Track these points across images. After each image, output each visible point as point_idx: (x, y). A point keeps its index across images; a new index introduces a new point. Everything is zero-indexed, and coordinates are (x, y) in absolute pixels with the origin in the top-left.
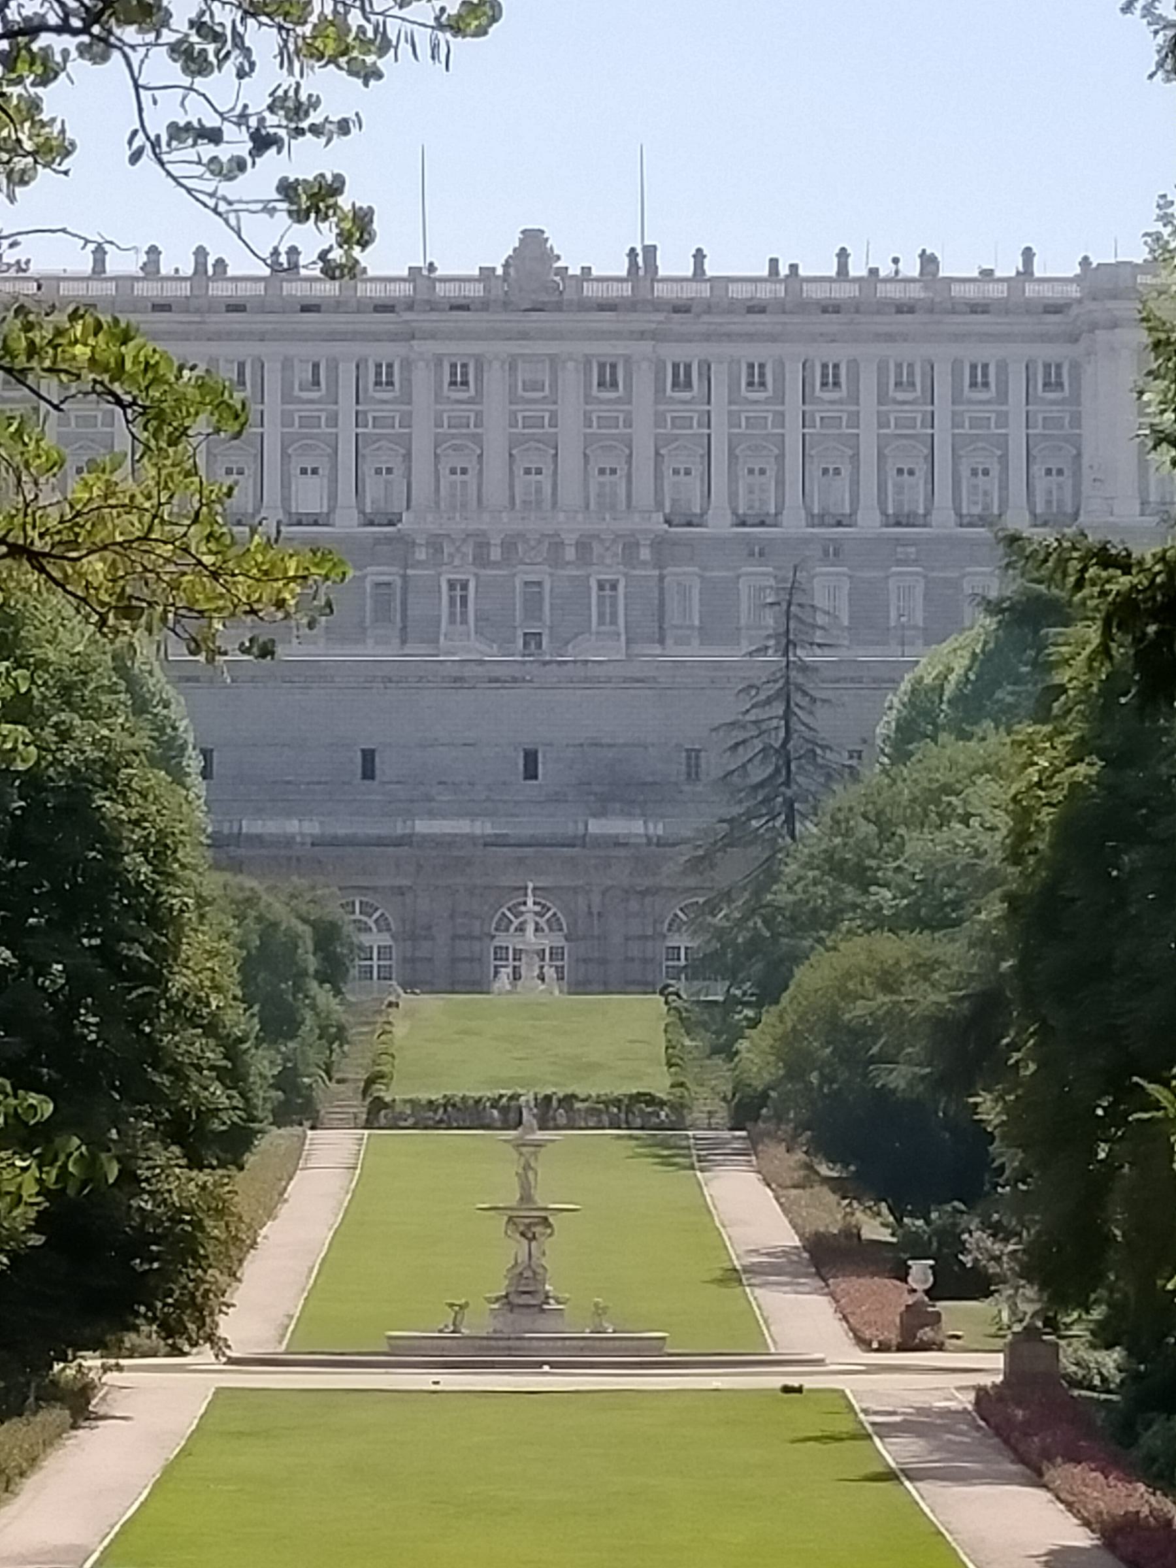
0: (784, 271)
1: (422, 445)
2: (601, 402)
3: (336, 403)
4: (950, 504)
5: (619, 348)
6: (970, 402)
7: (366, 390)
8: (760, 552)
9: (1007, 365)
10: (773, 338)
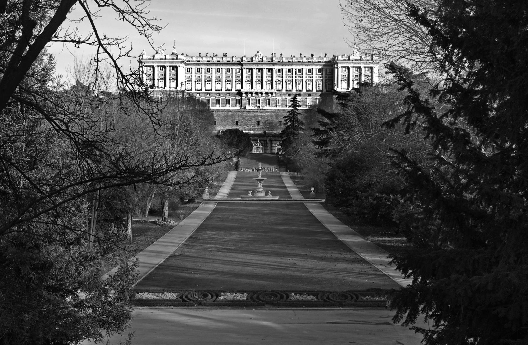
0: (293, 56)
8: (290, 95)
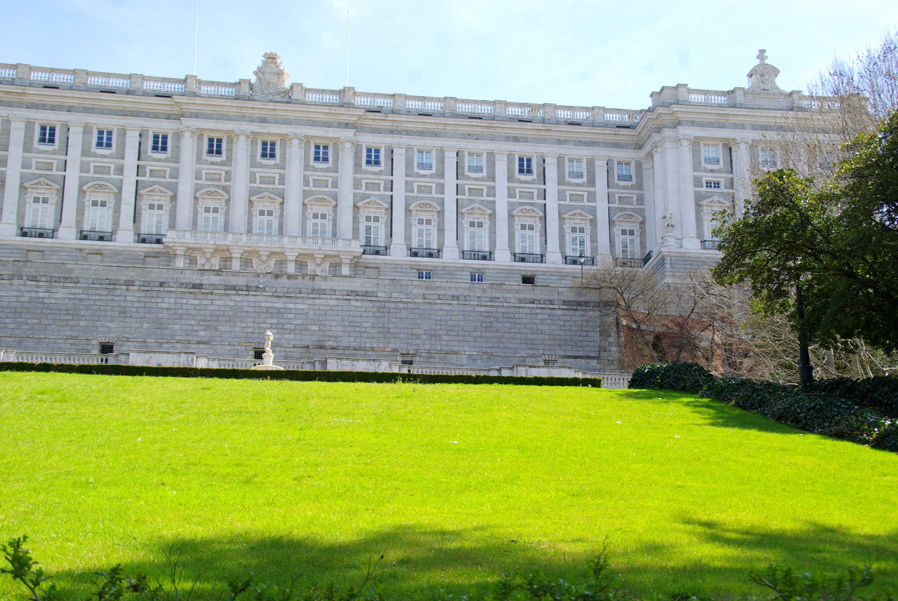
1: (186, 188)
2: (316, 170)
3: (123, 158)
4: (558, 250)
5: (332, 133)
6: (569, 184)
7: (146, 152)
9: (594, 162)
10: (436, 135)
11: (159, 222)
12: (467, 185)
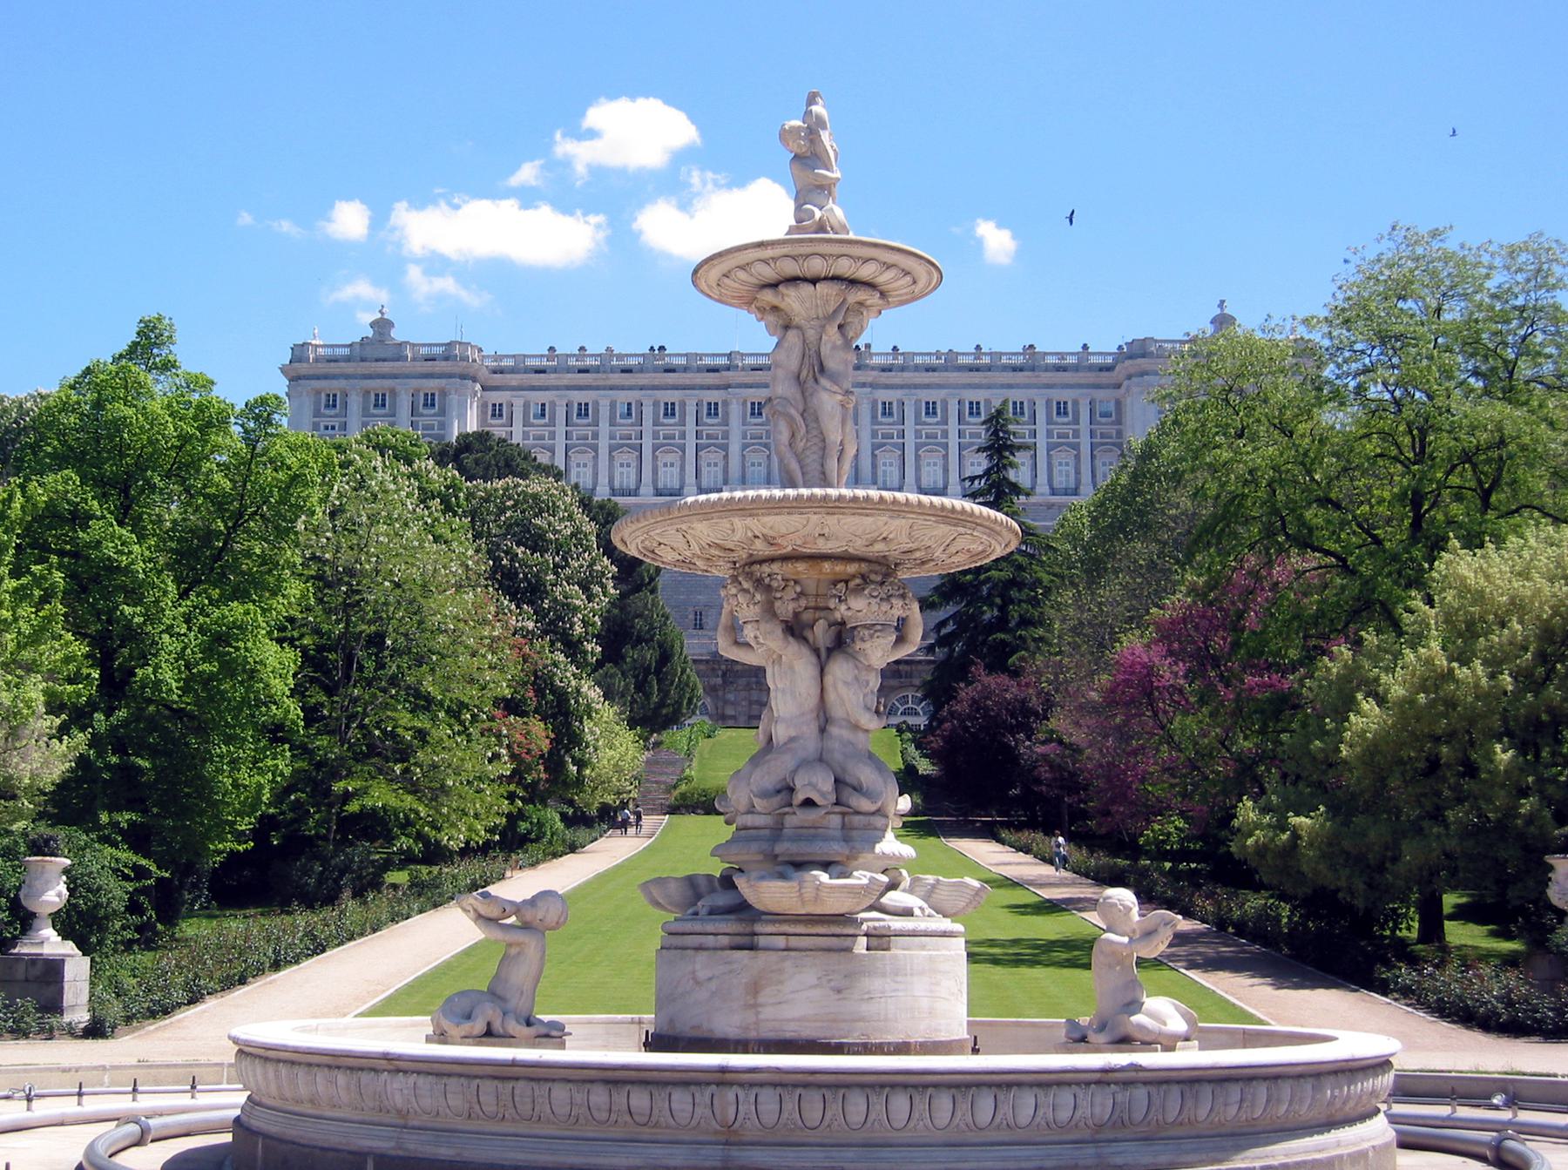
6: (1057, 424)
10: (940, 386)
11: (716, 477)
12: (968, 429)
